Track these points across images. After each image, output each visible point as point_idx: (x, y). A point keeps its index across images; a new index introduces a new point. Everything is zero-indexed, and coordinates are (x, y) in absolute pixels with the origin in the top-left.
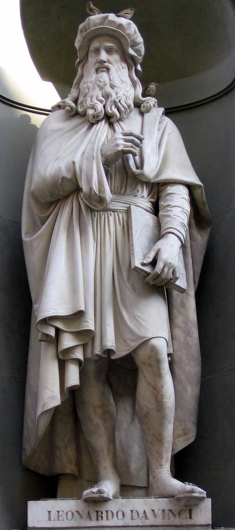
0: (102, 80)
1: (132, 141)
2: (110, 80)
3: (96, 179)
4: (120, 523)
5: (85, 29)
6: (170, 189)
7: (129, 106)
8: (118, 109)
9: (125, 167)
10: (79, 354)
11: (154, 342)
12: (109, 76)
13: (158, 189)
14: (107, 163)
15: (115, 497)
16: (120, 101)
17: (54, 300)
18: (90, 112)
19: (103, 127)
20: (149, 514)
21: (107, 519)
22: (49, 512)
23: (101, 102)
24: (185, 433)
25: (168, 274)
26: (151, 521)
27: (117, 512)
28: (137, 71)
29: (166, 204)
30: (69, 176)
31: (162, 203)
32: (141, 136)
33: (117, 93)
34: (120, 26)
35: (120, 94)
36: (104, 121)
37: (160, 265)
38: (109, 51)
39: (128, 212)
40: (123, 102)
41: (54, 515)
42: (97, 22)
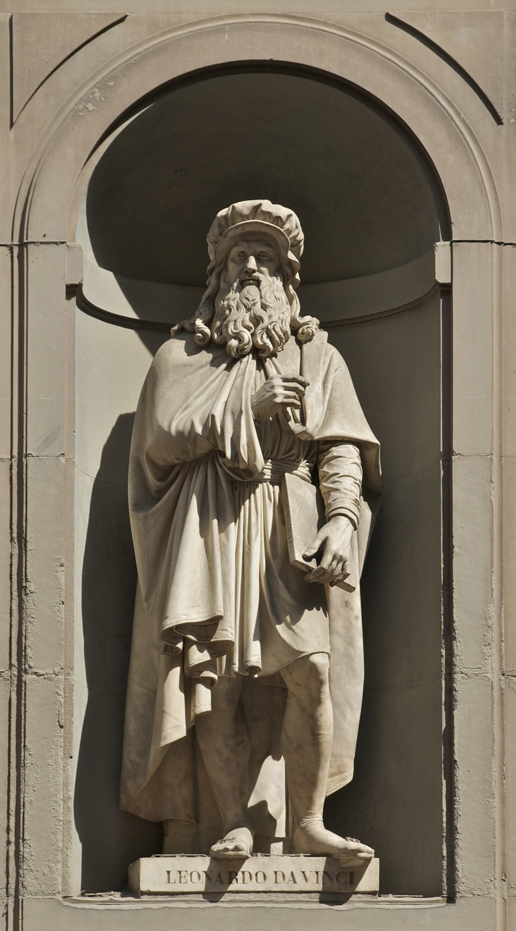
0: (250, 299)
2: (261, 297)
12: (260, 291)
16: (274, 329)
19: (249, 363)
20: (299, 877)
21: (244, 882)
22: (168, 872)
23: (248, 328)
27: (257, 874)
29: (331, 472)
32: (300, 378)
33: (270, 317)
34: (278, 219)
36: (251, 356)
40: (278, 329)
41: (174, 876)
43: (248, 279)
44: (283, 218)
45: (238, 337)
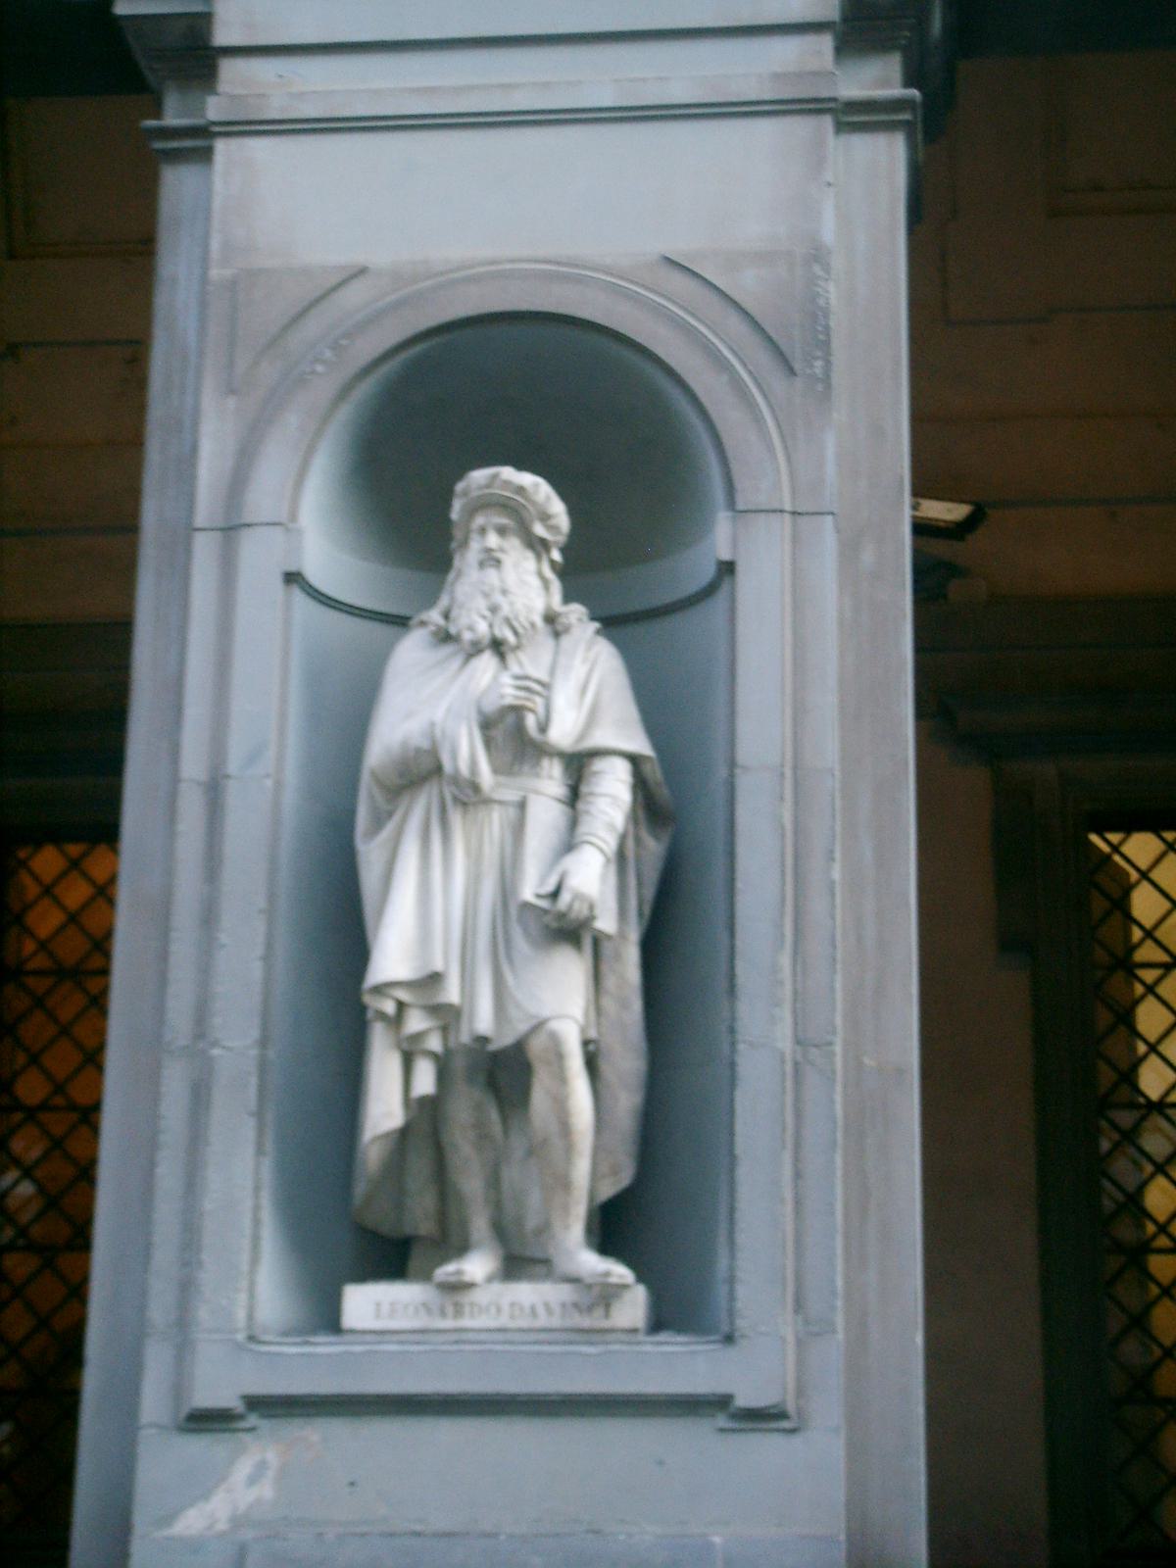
1: (528, 689)
3: (467, 751)
4: (492, 1323)
5: (465, 493)
6: (599, 765)
7: (533, 625)
8: (516, 633)
9: (520, 728)
10: (435, 1043)
11: (555, 1025)
13: (579, 765)
14: (487, 724)
15: (490, 1279)
17: (393, 957)
18: (467, 636)
19: (487, 661)
20: (541, 1311)
23: (484, 617)
24: (615, 1171)
25: (580, 910)
26: (543, 1321)
28: (552, 563)
30: (425, 745)
31: (584, 789)
35: (519, 606)
37: (565, 898)
38: (502, 531)
39: (522, 806)
40: (522, 619)
42: (483, 482)
43: (491, 560)
44: (528, 489)
45: (471, 628)
